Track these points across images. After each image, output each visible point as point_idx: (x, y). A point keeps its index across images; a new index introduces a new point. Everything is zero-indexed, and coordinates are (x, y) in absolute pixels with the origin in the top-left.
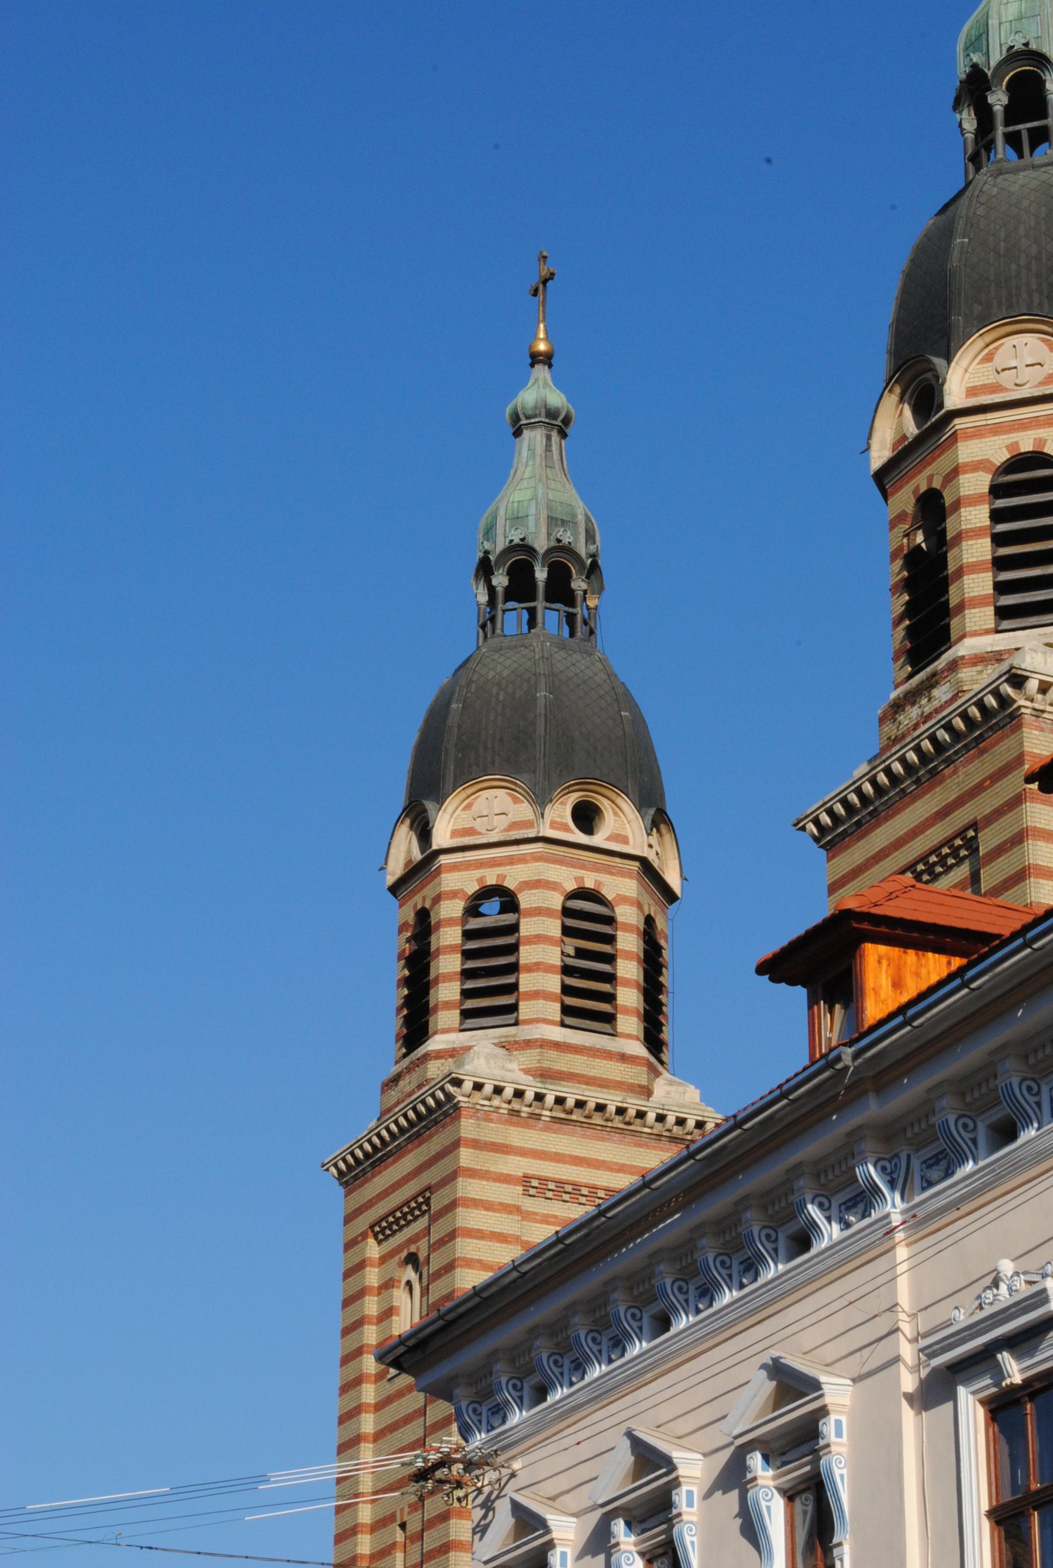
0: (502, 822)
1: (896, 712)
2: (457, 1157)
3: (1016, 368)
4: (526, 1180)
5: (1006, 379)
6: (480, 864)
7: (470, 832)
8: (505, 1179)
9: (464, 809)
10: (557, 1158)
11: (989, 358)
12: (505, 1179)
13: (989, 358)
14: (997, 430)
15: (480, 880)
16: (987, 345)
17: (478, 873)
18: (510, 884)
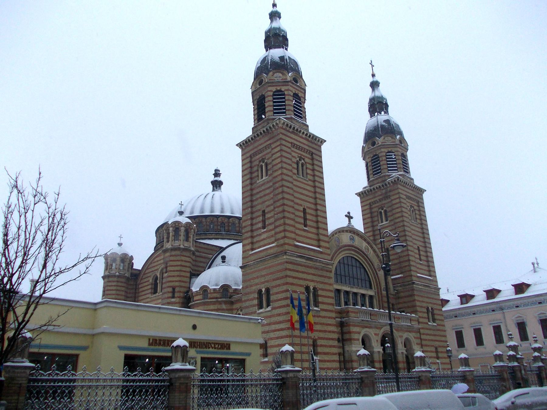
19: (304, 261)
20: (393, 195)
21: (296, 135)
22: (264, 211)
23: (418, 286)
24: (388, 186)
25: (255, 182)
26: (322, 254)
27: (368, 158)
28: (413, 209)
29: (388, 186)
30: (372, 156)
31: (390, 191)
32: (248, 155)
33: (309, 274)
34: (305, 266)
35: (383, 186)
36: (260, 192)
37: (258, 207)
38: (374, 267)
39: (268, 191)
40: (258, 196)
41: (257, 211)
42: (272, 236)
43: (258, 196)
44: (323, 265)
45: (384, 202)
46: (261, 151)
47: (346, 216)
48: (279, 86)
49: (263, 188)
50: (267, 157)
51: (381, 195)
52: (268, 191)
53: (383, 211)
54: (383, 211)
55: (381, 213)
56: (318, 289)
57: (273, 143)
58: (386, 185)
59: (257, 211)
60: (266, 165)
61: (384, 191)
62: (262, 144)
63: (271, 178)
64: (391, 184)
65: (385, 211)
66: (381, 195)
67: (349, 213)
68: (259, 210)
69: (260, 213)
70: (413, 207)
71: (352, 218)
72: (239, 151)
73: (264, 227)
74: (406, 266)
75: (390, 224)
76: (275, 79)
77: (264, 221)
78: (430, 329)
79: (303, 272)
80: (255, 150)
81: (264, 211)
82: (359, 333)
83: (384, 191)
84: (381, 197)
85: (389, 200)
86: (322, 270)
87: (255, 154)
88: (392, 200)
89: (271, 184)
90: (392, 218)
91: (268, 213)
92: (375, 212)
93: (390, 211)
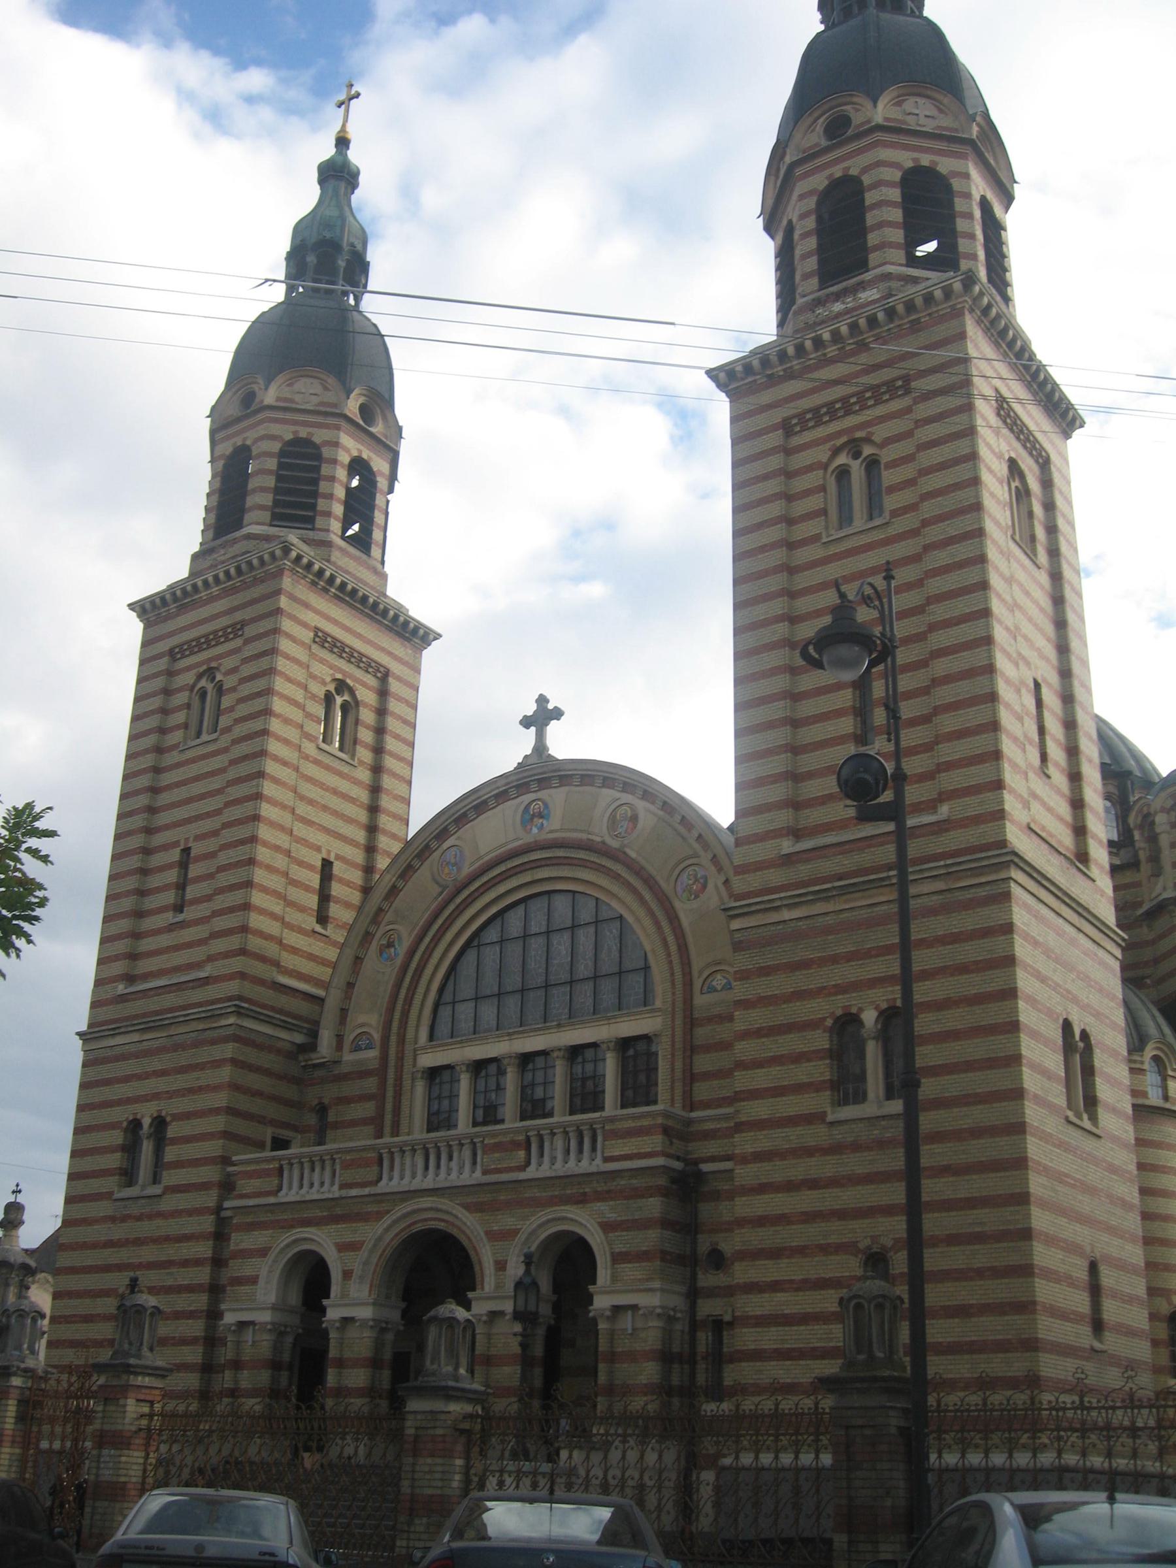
0: (315, 400)
1: (816, 307)
2: (279, 600)
3: (917, 115)
4: (317, 630)
5: (909, 119)
6: (295, 423)
7: (292, 401)
8: (305, 625)
9: (288, 385)
10: (335, 622)
11: (899, 104)
12: (305, 625)
13: (899, 104)
14: (906, 147)
15: (295, 432)
16: (898, 97)
17: (293, 428)
18: (317, 439)
19: (136, 1037)
21: (194, 605)
23: (775, 917)
26: (207, 984)
28: (867, 450)
33: (146, 1076)
34: (137, 1055)
44: (201, 1026)
47: (526, 722)
56: (168, 1119)
67: (542, 700)
70: (868, 440)
71: (557, 714)
78: (836, 1149)
79: (127, 1079)
82: (263, 1252)
86: (197, 1044)
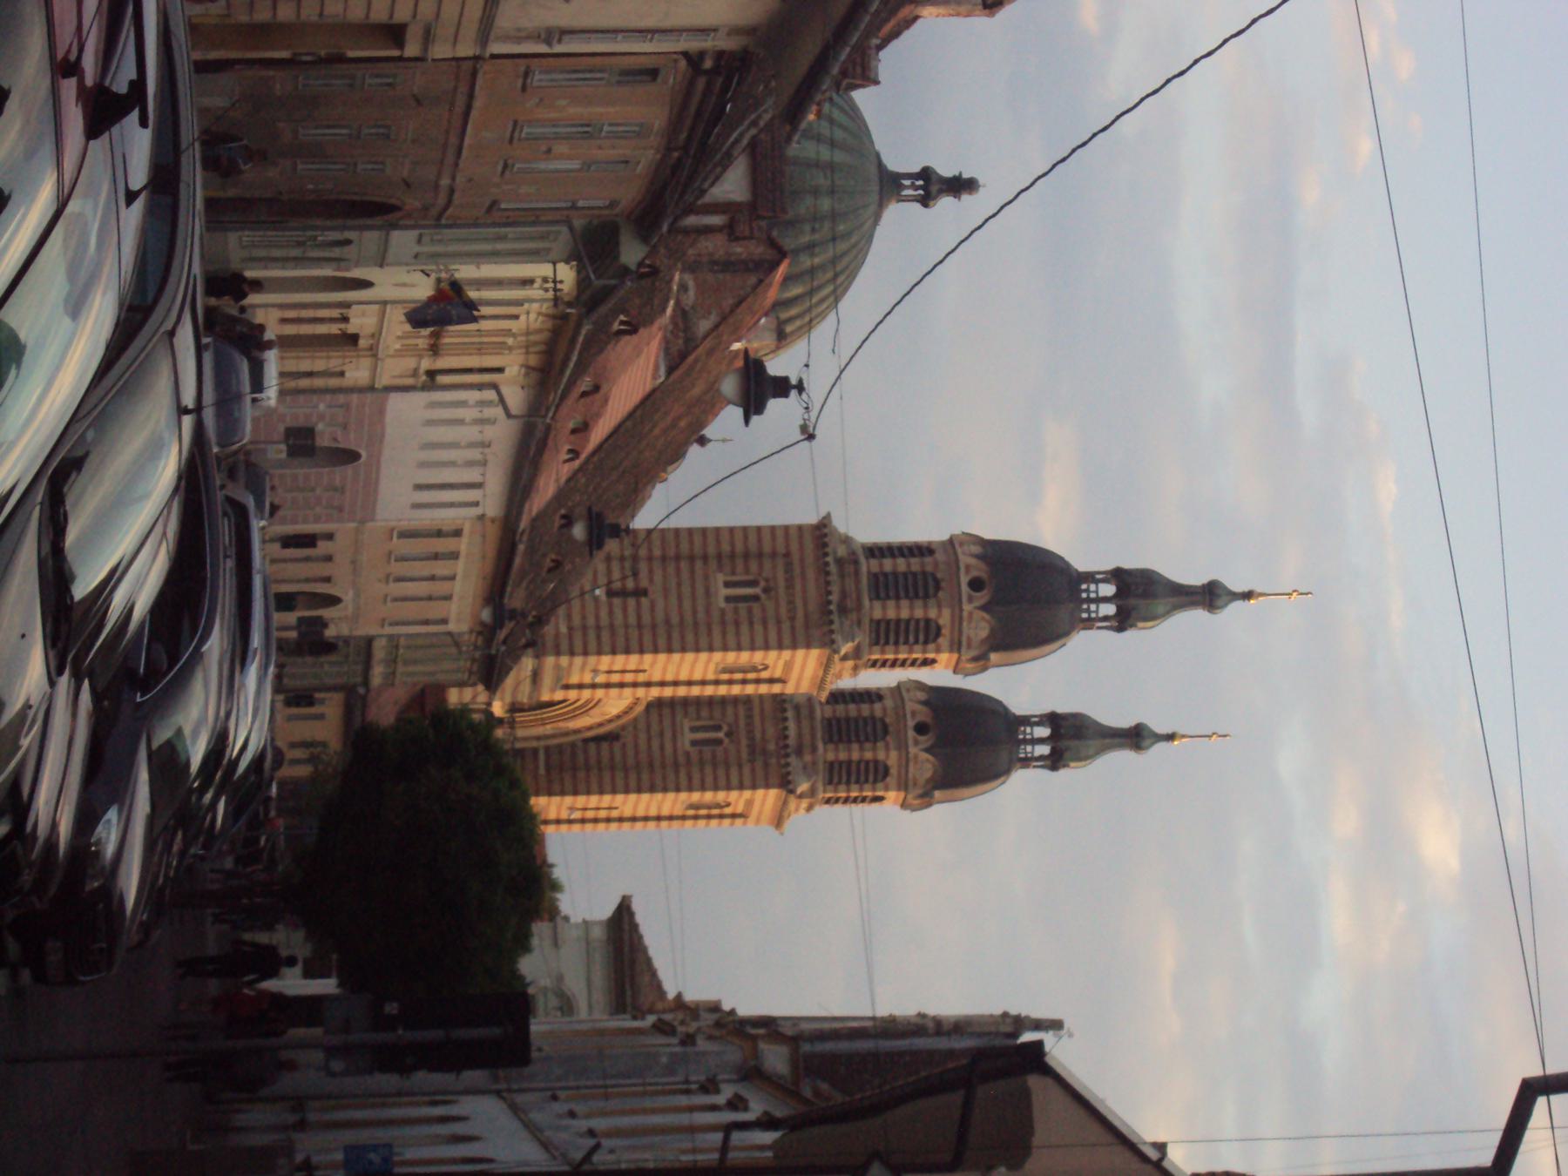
20: (753, 770)
22: (645, 593)
24: (783, 762)
25: (720, 568)
27: (884, 710)
29: (783, 762)
30: (888, 720)
31: (766, 765)
32: (794, 547)
35: (786, 746)
36: (693, 587)
37: (658, 577)
38: (559, 721)
39: (687, 604)
40: (685, 575)
41: (651, 571)
42: (584, 618)
43: (685, 575)
45: (744, 742)
46: (790, 585)
48: (952, 632)
49: (700, 591)
50: (770, 605)
51: (764, 732)
52: (687, 604)
53: (721, 735)
54: (721, 735)
55: (718, 728)
57: (793, 628)
58: (787, 755)
59: (651, 571)
60: (756, 598)
61: (771, 747)
62: (804, 591)
63: (716, 615)
64: (784, 771)
65: (719, 742)
66: (764, 732)
68: (651, 580)
69: (644, 583)
72: (812, 519)
73: (611, 593)
74: (562, 784)
75: (680, 752)
76: (973, 625)
77: (623, 593)
80: (797, 571)
81: (645, 593)
83: (771, 747)
84: (758, 735)
85: (744, 755)
87: (789, 568)
88: (740, 766)
89: (701, 615)
90: (694, 756)
91: (639, 605)
92: (724, 714)
93: (714, 756)
